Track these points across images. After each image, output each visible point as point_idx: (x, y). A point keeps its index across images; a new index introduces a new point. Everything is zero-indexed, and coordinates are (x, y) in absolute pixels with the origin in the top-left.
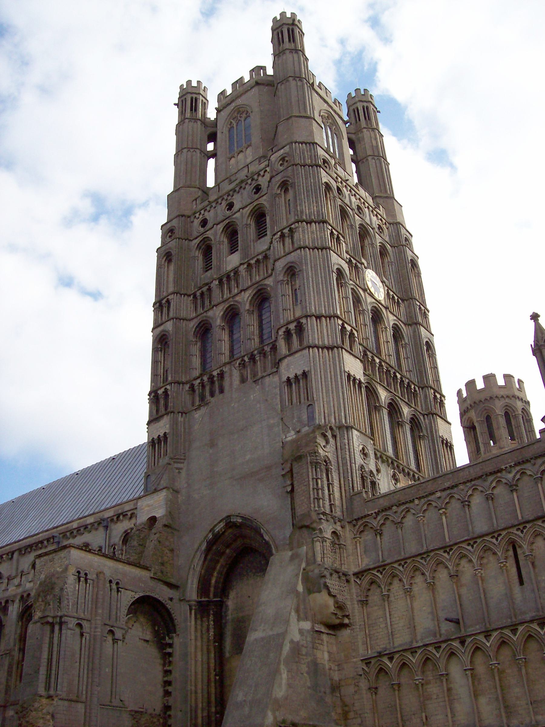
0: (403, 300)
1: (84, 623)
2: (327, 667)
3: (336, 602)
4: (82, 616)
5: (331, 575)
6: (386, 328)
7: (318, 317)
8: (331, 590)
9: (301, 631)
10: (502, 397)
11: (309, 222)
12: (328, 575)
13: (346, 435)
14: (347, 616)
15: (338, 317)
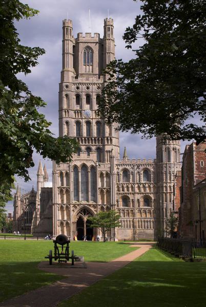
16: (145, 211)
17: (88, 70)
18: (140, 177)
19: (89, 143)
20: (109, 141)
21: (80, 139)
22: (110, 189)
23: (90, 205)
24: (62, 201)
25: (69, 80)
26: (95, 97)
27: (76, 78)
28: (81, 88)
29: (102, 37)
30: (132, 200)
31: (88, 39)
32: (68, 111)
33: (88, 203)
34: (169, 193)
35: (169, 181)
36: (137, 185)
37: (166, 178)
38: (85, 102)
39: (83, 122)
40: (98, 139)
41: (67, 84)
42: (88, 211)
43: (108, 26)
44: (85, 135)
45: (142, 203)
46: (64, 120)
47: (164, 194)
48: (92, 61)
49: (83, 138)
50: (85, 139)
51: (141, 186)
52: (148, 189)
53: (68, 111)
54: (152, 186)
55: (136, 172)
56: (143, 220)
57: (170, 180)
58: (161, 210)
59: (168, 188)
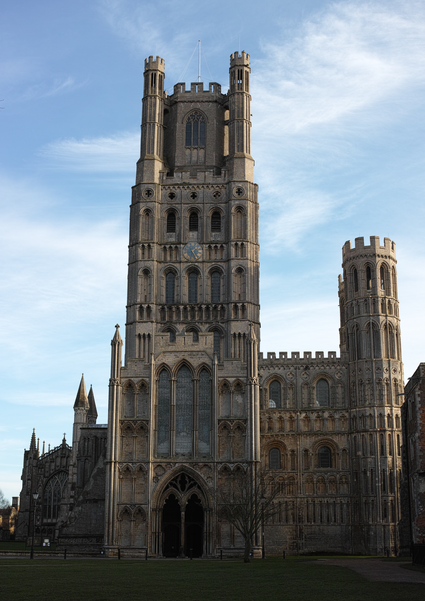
4: (89, 454)
15: (136, 304)
17: (194, 159)
18: (310, 394)
19: (193, 317)
20: (240, 312)
21: (174, 309)
22: (245, 421)
23: (196, 464)
25: (153, 178)
26: (210, 214)
27: (170, 174)
28: (179, 196)
29: (225, 90)
30: (293, 451)
36: (304, 415)
37: (373, 395)
38: (187, 227)
39: (182, 268)
40: (215, 308)
42: (190, 479)
43: (240, 68)
44: (185, 299)
45: (313, 461)
46: (141, 265)
47: (367, 436)
48: (204, 143)
49: (182, 307)
50: (185, 308)
51: (313, 416)
53: (149, 246)
54: (337, 416)
55: (300, 381)
56: (317, 501)
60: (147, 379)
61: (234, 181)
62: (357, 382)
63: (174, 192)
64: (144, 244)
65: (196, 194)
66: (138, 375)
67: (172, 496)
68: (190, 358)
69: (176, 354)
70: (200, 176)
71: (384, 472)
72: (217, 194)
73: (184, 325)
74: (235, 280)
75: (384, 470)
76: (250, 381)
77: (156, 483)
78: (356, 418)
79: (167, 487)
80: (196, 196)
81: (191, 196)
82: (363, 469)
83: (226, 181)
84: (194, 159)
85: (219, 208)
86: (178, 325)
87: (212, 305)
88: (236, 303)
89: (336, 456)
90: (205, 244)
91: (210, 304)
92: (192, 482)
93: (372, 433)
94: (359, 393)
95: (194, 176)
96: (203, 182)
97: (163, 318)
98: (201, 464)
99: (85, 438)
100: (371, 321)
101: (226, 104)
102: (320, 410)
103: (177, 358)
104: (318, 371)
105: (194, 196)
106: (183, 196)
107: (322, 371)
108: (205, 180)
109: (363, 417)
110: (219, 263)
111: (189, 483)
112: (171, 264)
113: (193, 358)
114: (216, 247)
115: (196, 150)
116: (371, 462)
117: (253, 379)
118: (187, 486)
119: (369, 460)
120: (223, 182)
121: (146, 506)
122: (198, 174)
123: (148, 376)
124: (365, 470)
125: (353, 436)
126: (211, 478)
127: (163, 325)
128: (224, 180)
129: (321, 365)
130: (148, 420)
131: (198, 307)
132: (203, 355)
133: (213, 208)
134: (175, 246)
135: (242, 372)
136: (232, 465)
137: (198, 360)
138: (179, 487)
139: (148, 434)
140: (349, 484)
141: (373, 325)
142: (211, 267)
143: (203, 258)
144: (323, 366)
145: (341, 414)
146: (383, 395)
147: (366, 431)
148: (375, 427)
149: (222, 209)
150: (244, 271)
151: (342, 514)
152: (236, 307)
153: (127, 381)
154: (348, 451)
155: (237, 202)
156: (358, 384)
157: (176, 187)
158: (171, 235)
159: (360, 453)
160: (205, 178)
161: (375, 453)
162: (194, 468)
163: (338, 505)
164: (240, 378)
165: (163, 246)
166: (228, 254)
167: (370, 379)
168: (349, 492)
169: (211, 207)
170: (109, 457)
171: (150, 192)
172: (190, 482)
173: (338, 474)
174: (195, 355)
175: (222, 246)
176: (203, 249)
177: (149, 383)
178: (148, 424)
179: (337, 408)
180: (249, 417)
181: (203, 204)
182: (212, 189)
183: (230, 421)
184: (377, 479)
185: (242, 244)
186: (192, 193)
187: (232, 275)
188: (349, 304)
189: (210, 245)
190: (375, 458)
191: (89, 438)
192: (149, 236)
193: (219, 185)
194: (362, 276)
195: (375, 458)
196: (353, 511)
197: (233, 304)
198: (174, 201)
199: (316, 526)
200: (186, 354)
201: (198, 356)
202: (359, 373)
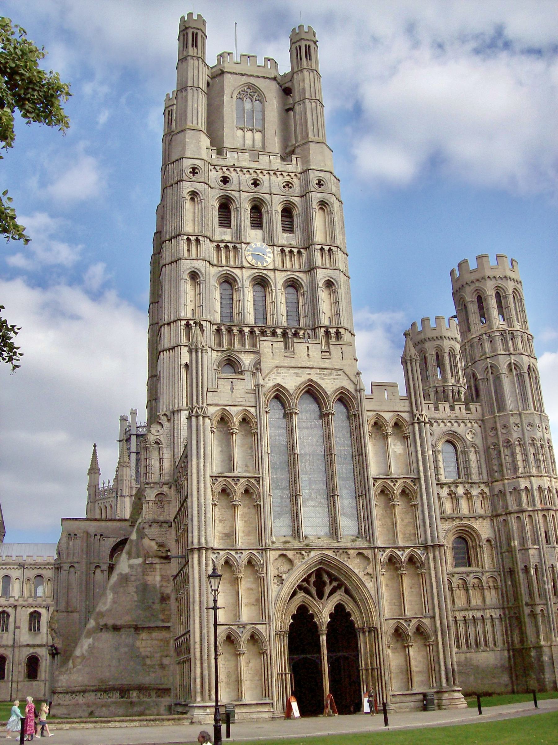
0: (305, 248)
1: (76, 565)
2: (158, 586)
3: (157, 543)
4: (76, 560)
5: (150, 526)
6: (271, 290)
7: (169, 324)
8: (149, 536)
9: (131, 567)
10: (472, 282)
11: (170, 240)
12: (147, 526)
13: (176, 417)
14: (169, 551)
15: (181, 320)
16: (465, 582)
17: (249, 142)
23: (345, 550)
24: (230, 535)
28: (236, 181)
31: (246, 68)
32: (197, 240)
33: (335, 545)
34: (543, 510)
35: (534, 471)
37: (526, 460)
38: (248, 222)
41: (197, 162)
42: (333, 578)
44: (250, 319)
49: (247, 330)
50: (252, 332)
52: (464, 504)
53: (197, 240)
54: (475, 492)
56: (459, 616)
57: (538, 467)
58: (522, 575)
59: (536, 495)
60: (252, 410)
61: (313, 169)
62: (501, 443)
63: (228, 176)
64: (190, 237)
65: (258, 182)
66: (237, 403)
67: (303, 609)
68: (320, 378)
69: (296, 370)
70: (264, 159)
71: (553, 568)
72: (288, 185)
73: (252, 355)
74: (323, 296)
75: (552, 565)
76: (418, 418)
77: (278, 585)
78: (505, 494)
79: (294, 594)
80: (258, 185)
81: (252, 184)
82: (523, 567)
83: (299, 170)
84: (249, 142)
85: (291, 202)
86: (243, 355)
87: (291, 330)
88: (327, 328)
89: (478, 550)
90: (276, 246)
91: (287, 328)
92: (335, 584)
93: (531, 513)
94: (505, 458)
95: (255, 159)
96: (267, 168)
97: (220, 344)
98: (351, 552)
99: (70, 534)
100: (512, 361)
101: (287, 85)
102: (453, 483)
103: (299, 378)
104: (445, 429)
105: (256, 183)
106: (241, 182)
107: (449, 429)
108: (270, 166)
109: (516, 490)
110: (297, 274)
111: (331, 583)
112: (228, 268)
113: (323, 379)
114: (291, 252)
115: (250, 132)
116: (533, 555)
117: (422, 415)
118: (328, 589)
119: (531, 552)
120: (295, 171)
121: (264, 626)
122: (261, 157)
123: (253, 404)
124: (526, 566)
125: (501, 519)
126: (371, 574)
127: (220, 354)
128: (297, 168)
129: (448, 421)
130: (259, 478)
131: (271, 332)
132: (340, 375)
133: (283, 201)
134: (232, 245)
135: (402, 404)
136: (401, 552)
137: (333, 382)
138: (314, 591)
139: (260, 501)
140: (499, 590)
141: (515, 368)
142: (286, 278)
143: (274, 264)
144: (450, 422)
145: (480, 489)
146: (539, 460)
147: (523, 511)
148: (534, 505)
149: (296, 203)
150: (336, 285)
151: (494, 633)
152: (327, 333)
153: (218, 410)
154: (493, 542)
155: (319, 195)
156: (503, 446)
157: (232, 169)
158: (224, 232)
159: (516, 543)
160: (270, 162)
161: (538, 541)
162: (340, 557)
163: (487, 621)
164: (399, 413)
165: (215, 244)
166: (311, 261)
167: (520, 438)
168: (499, 602)
169: (282, 200)
170: (196, 541)
171: (197, 170)
172: (331, 583)
173: (483, 575)
174: (327, 374)
175: (299, 252)
176: (273, 253)
177: (256, 415)
178: (259, 484)
179: (473, 481)
180: (422, 474)
181: (270, 194)
182: (280, 177)
183: (392, 481)
184: (545, 579)
185: (330, 250)
186: (254, 179)
187: (319, 289)
188: (476, 340)
189: (282, 249)
190: (539, 549)
191: (75, 535)
192: (196, 228)
193: (290, 174)
194: (493, 303)
195: (539, 549)
196: (509, 628)
197: (323, 330)
198: (227, 187)
199: (461, 654)
200: (313, 372)
201: (332, 377)
202: (503, 431)
